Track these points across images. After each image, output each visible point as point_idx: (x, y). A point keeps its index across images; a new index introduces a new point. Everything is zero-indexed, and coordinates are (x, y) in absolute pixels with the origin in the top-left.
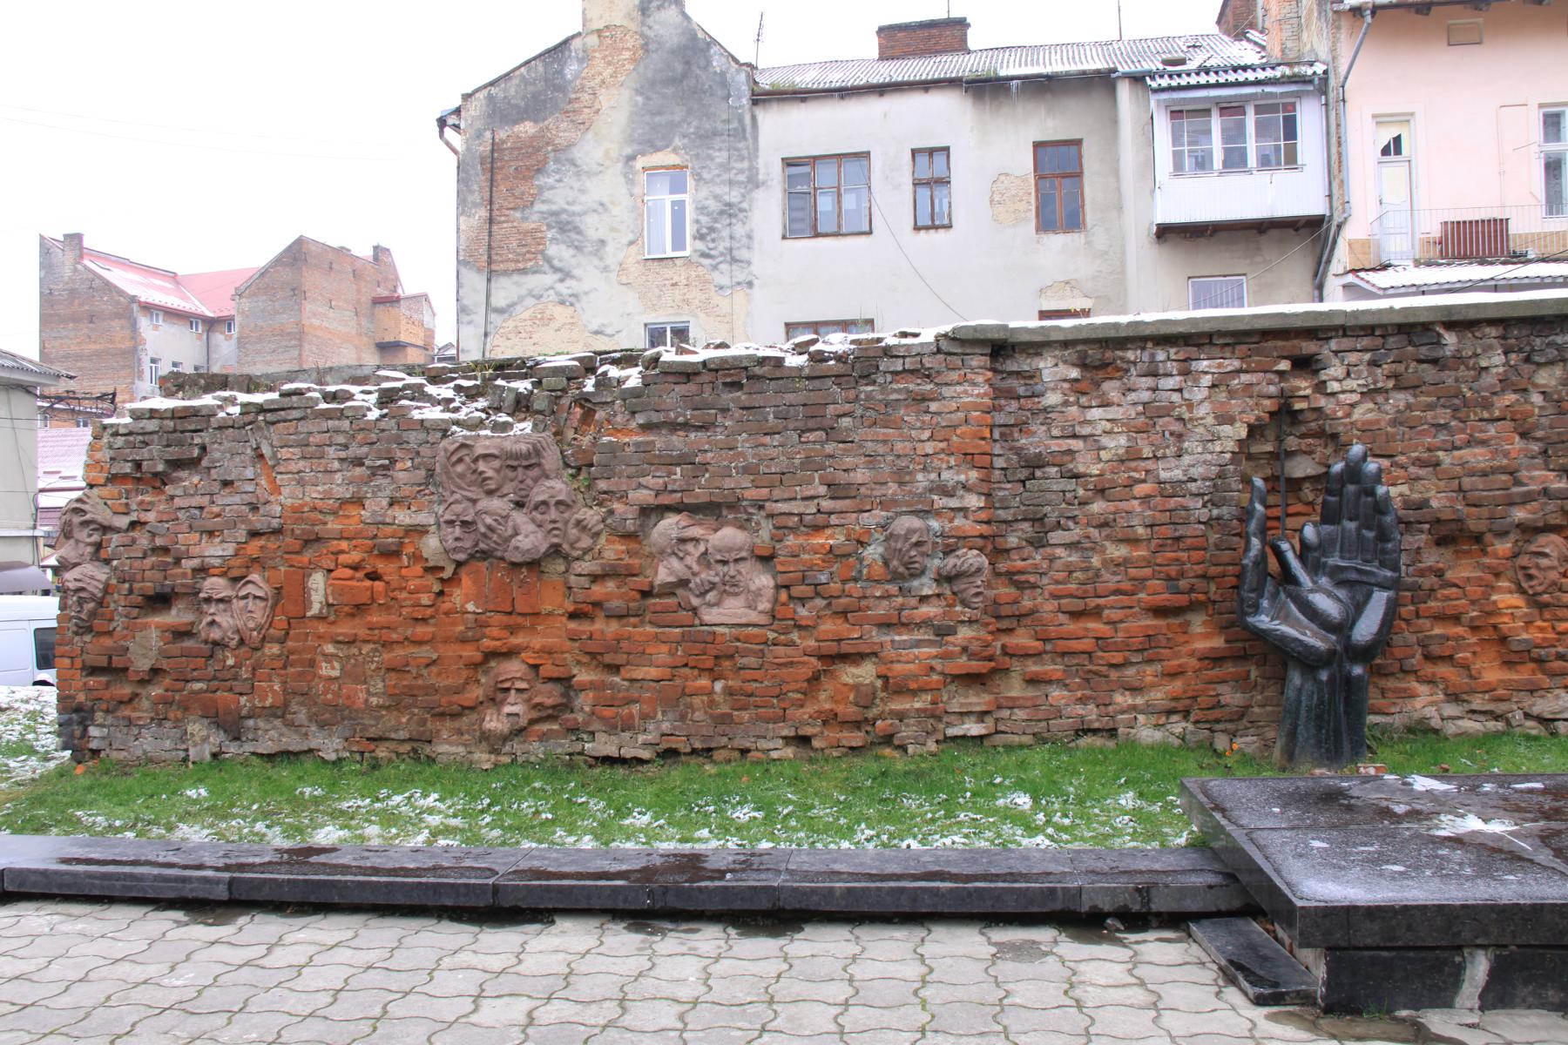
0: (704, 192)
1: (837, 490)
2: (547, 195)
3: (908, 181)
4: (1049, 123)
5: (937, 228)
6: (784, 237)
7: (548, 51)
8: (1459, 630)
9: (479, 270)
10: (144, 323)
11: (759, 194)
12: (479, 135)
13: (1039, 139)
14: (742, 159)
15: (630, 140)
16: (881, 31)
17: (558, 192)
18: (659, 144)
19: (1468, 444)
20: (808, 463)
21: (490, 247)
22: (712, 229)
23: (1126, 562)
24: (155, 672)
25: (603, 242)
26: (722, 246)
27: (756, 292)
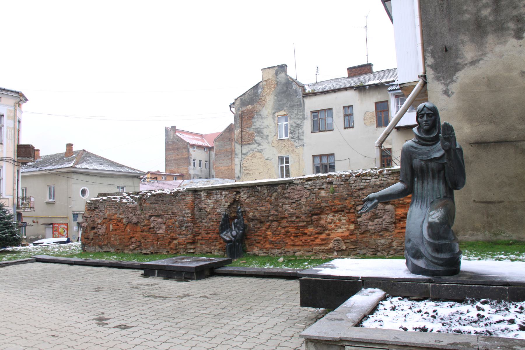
0: (292, 122)
1: (173, 213)
2: (255, 124)
3: (342, 115)
4: (378, 97)
5: (350, 128)
6: (312, 132)
7: (254, 87)
8: (261, 238)
9: (239, 144)
10: (191, 150)
11: (305, 121)
12: (239, 109)
13: (376, 101)
14: (301, 112)
15: (274, 109)
16: (348, 69)
17: (257, 123)
18: (281, 109)
19: (262, 206)
20: (169, 209)
21: (242, 138)
22: (294, 131)
23: (212, 225)
24: (92, 239)
25: (268, 136)
26: (296, 135)
27: (305, 147)
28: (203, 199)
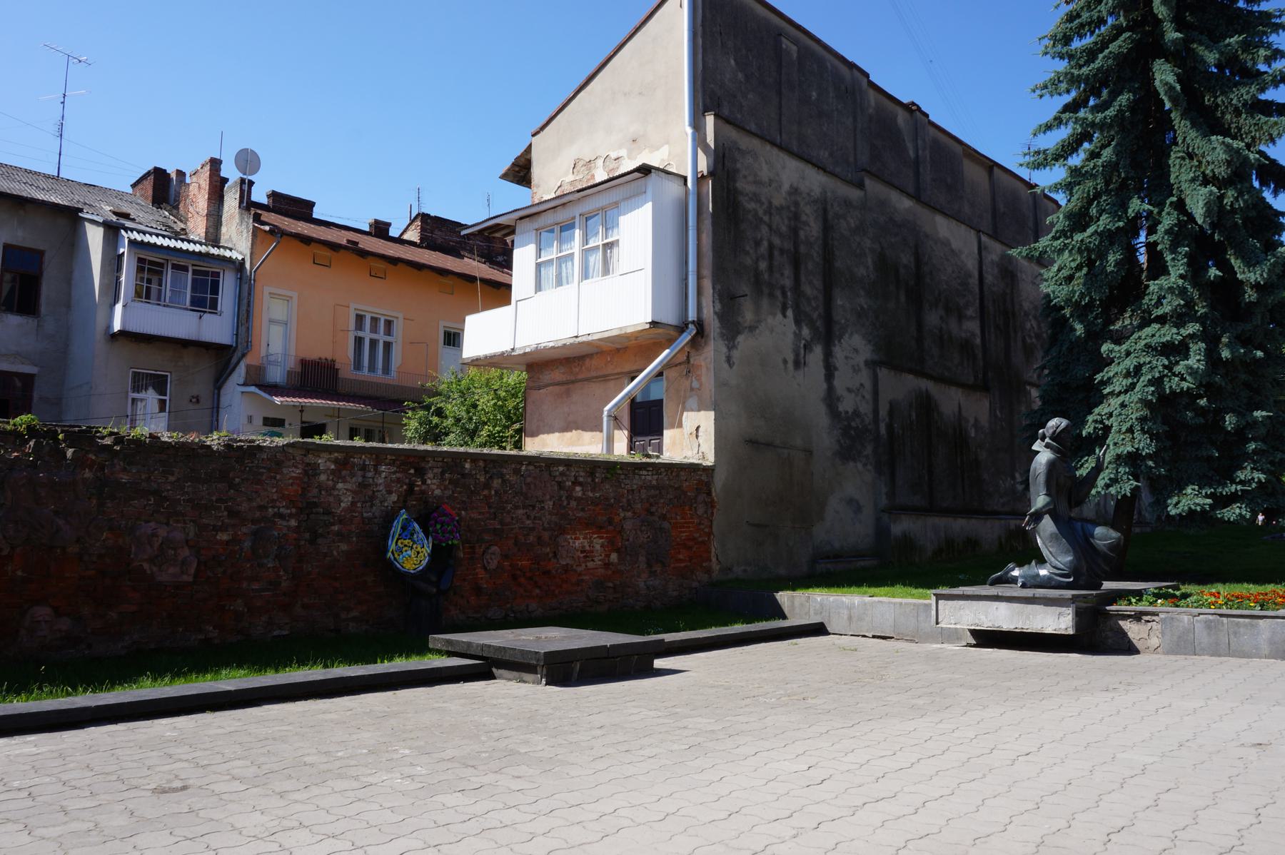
1: (232, 513)
28: (323, 477)
